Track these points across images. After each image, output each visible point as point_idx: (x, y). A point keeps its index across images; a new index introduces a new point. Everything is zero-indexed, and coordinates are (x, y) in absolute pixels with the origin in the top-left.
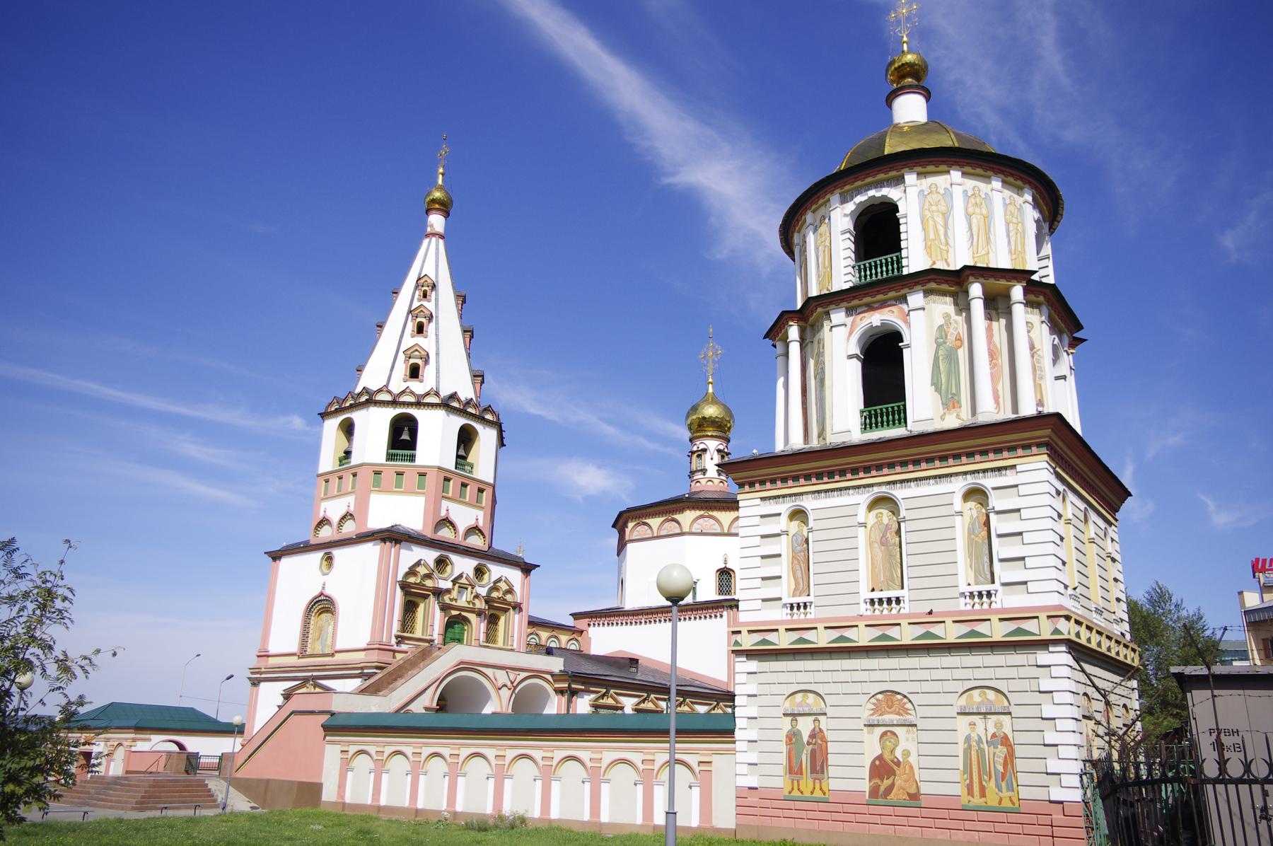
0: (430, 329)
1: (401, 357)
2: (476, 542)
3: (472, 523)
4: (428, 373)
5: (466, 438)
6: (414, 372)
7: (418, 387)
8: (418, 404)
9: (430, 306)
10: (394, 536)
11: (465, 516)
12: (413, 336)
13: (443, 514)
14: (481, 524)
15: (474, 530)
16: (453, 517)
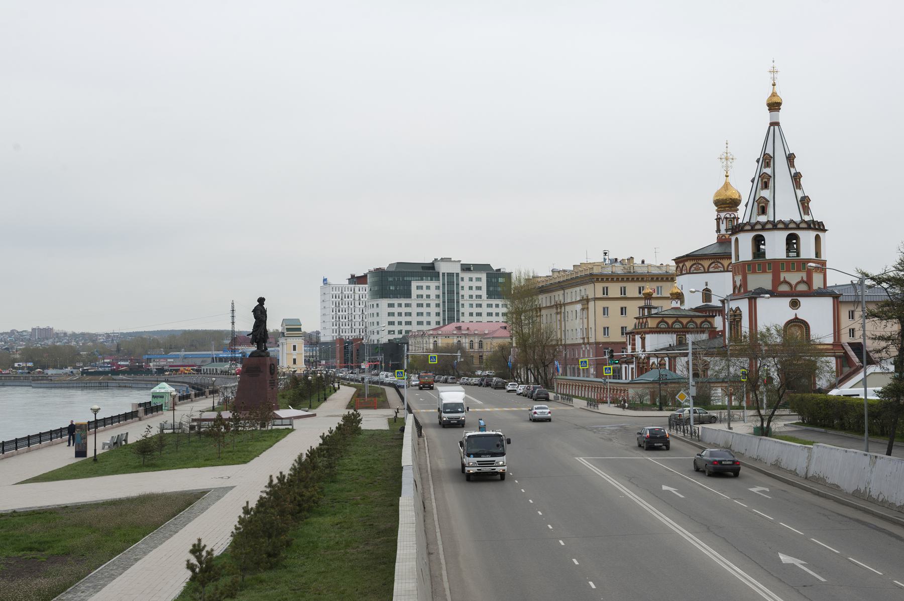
0: (771, 184)
1: (756, 204)
2: (803, 288)
3: (800, 279)
4: (770, 210)
5: (792, 241)
6: (763, 211)
7: (763, 219)
8: (764, 229)
9: (768, 171)
10: (760, 292)
11: (793, 277)
12: (762, 189)
13: (782, 279)
14: (805, 279)
15: (802, 281)
16: (787, 279)
